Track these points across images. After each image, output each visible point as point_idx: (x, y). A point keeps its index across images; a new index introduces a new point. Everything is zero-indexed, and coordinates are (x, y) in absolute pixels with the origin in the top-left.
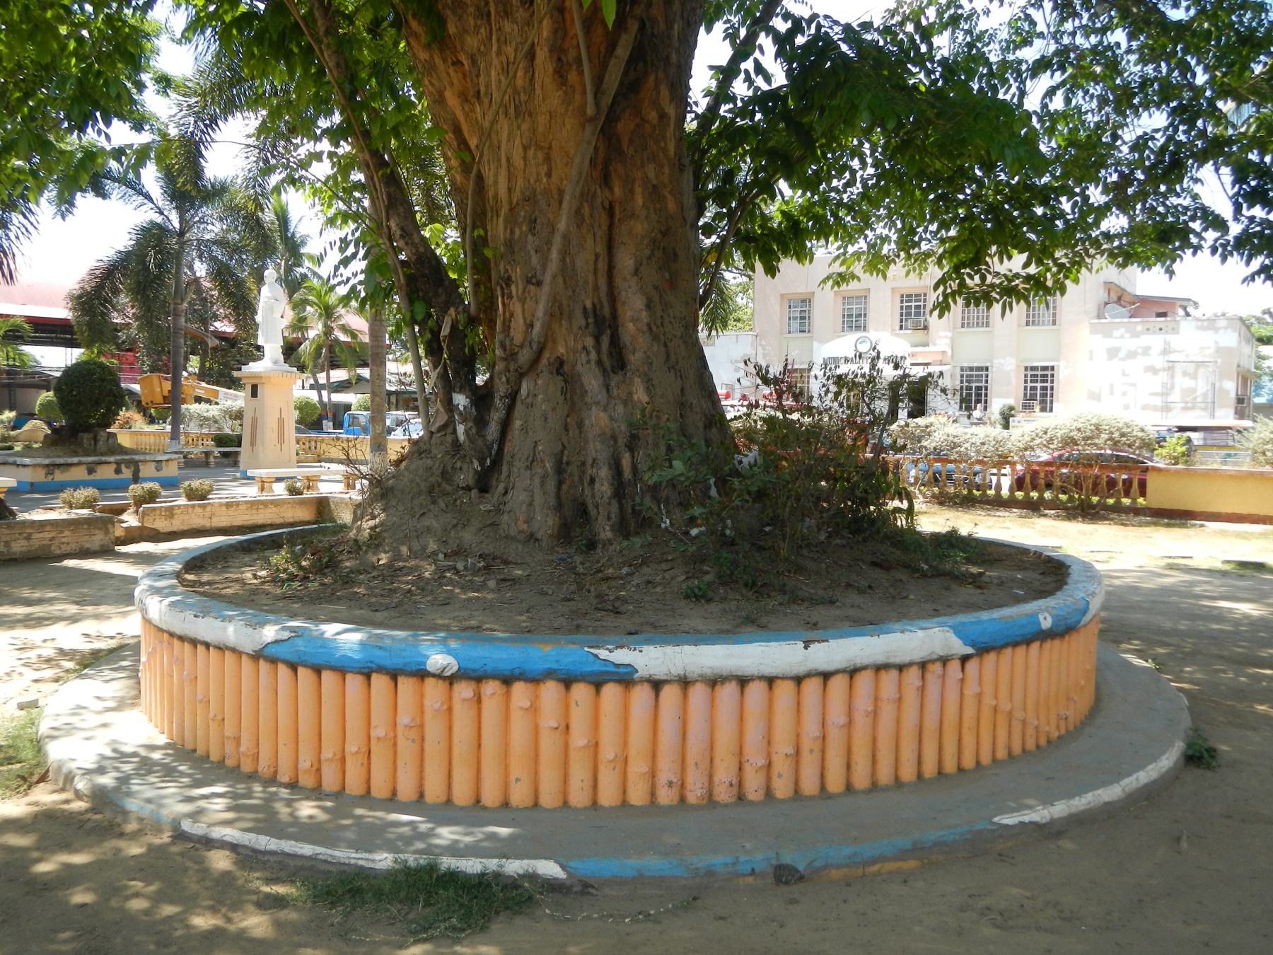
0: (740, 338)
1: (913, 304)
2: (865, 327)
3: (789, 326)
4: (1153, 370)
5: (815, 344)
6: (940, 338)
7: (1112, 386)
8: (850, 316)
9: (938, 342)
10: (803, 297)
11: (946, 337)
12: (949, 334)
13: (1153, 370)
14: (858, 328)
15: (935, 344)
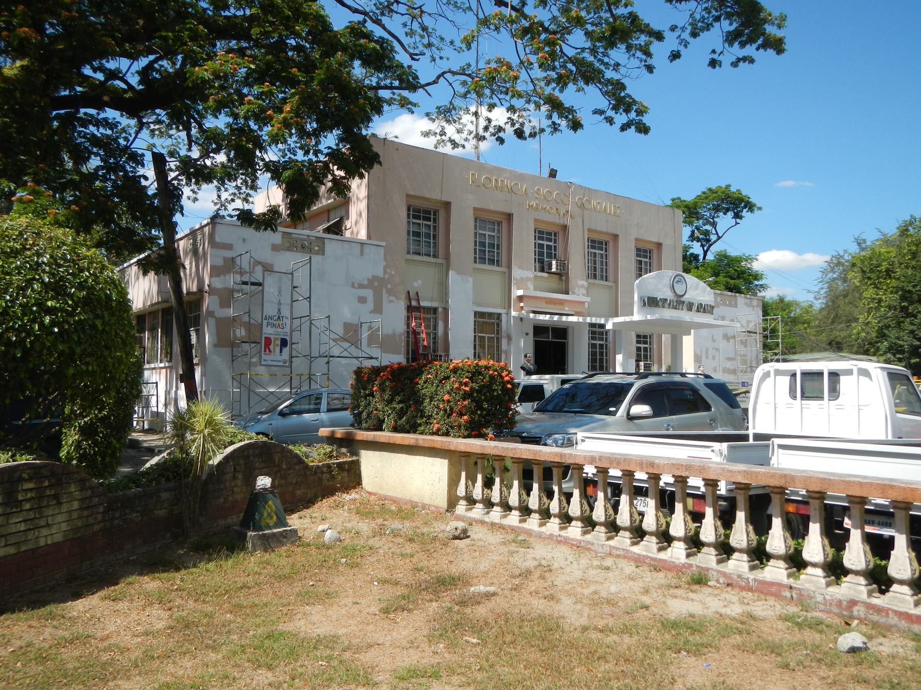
0: (367, 249)
1: (545, 243)
2: (498, 261)
3: (408, 244)
4: (727, 337)
5: (451, 273)
6: (579, 287)
7: (707, 350)
8: (483, 244)
9: (576, 290)
10: (427, 205)
11: (583, 286)
12: (585, 283)
13: (727, 337)
14: (492, 262)
15: (574, 293)
